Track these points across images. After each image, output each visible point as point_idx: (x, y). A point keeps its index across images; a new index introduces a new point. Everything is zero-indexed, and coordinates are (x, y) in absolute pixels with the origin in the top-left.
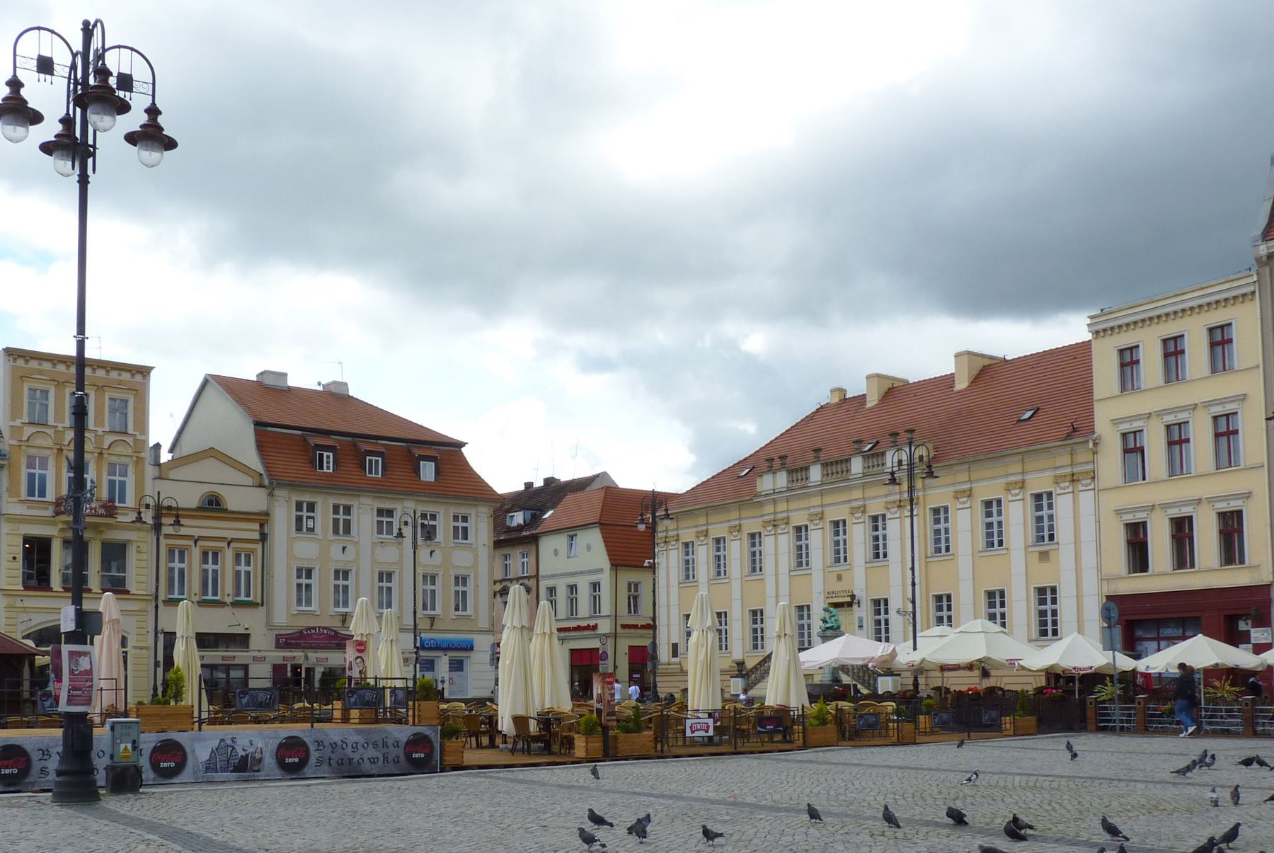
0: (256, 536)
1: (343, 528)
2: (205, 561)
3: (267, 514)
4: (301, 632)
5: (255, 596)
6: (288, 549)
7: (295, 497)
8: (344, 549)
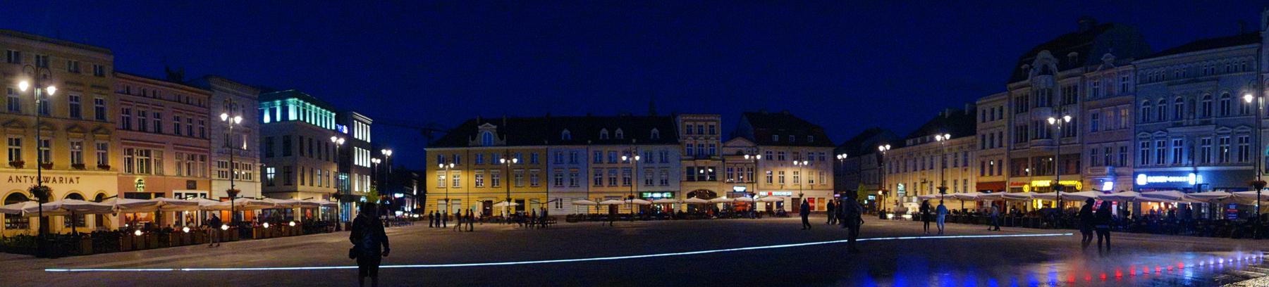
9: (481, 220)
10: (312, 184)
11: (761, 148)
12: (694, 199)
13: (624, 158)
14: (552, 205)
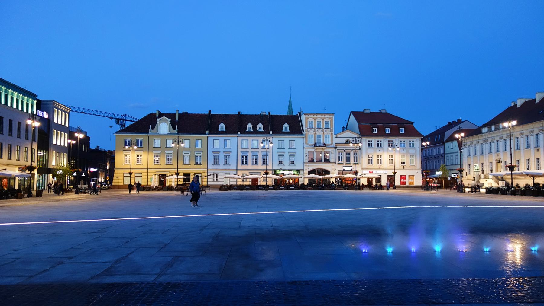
1: (379, 145)
9: (156, 189)
10: (9, 158)
11: (364, 139)
12: (313, 176)
13: (262, 145)
14: (211, 178)
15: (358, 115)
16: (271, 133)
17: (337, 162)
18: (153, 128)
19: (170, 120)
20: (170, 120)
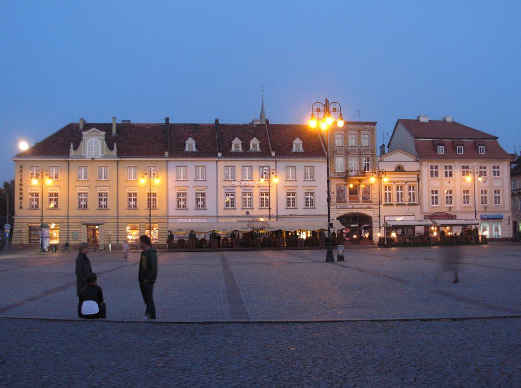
0: (416, 179)
2: (398, 190)
3: (420, 171)
4: (434, 214)
5: (416, 202)
6: (428, 183)
7: (430, 164)
8: (449, 182)
11: (424, 163)
15: (412, 126)
16: (273, 154)
17: (383, 202)
18: (75, 148)
19: (104, 133)
20: (104, 133)
